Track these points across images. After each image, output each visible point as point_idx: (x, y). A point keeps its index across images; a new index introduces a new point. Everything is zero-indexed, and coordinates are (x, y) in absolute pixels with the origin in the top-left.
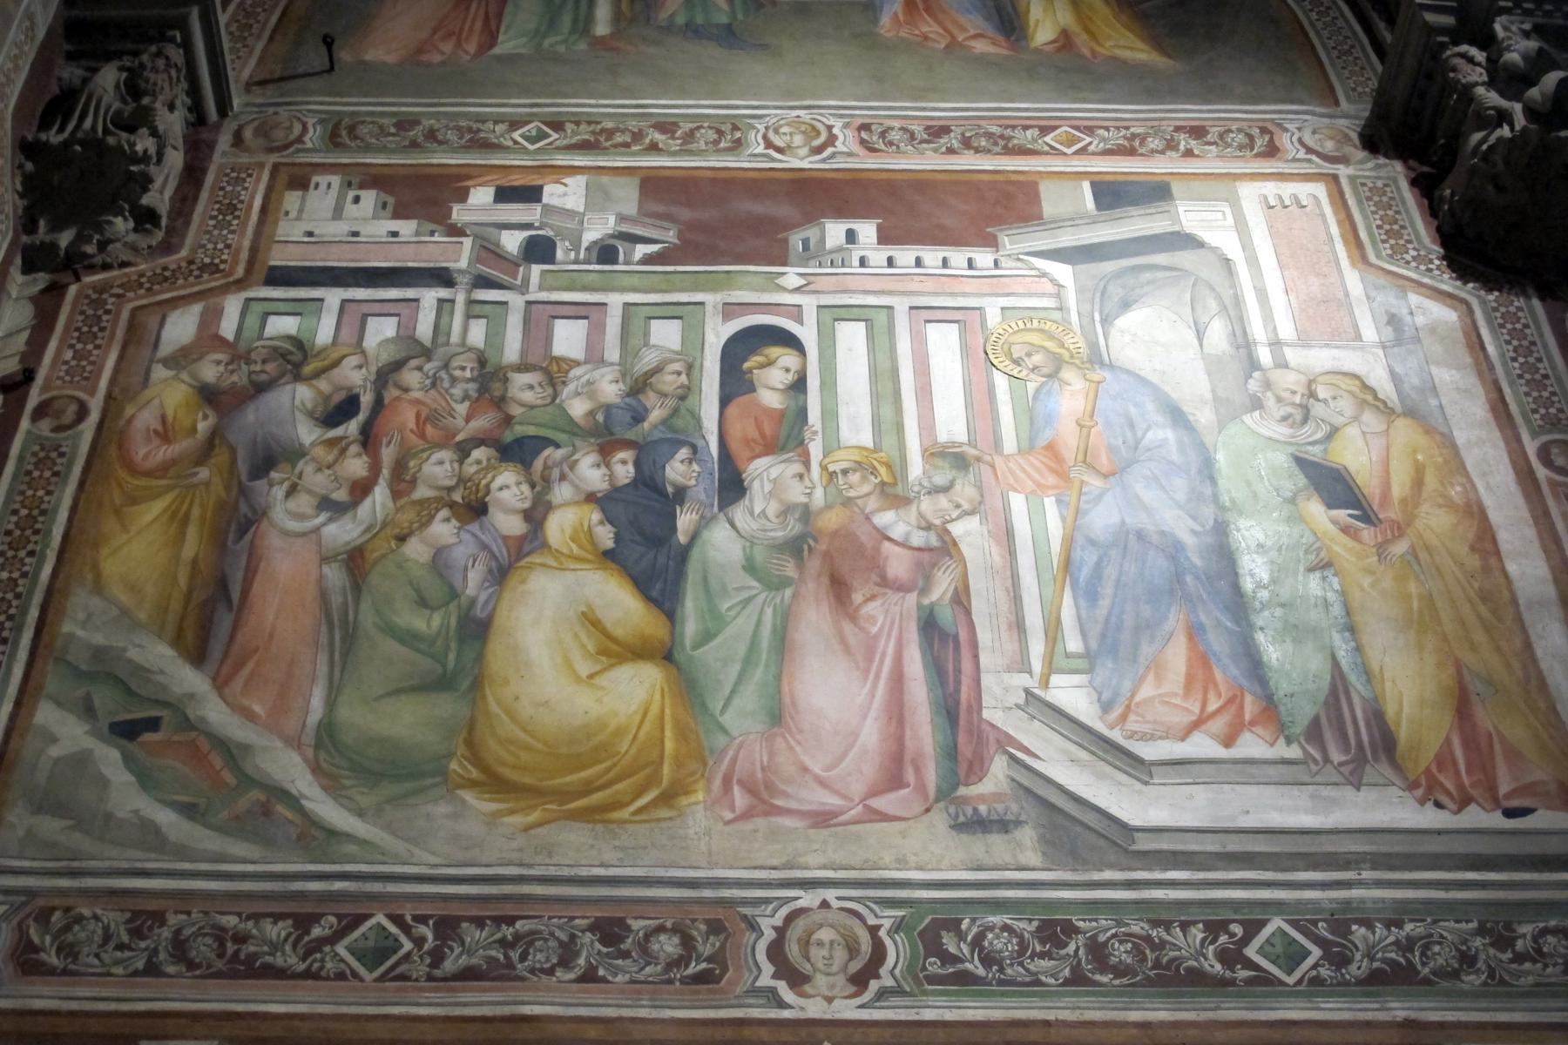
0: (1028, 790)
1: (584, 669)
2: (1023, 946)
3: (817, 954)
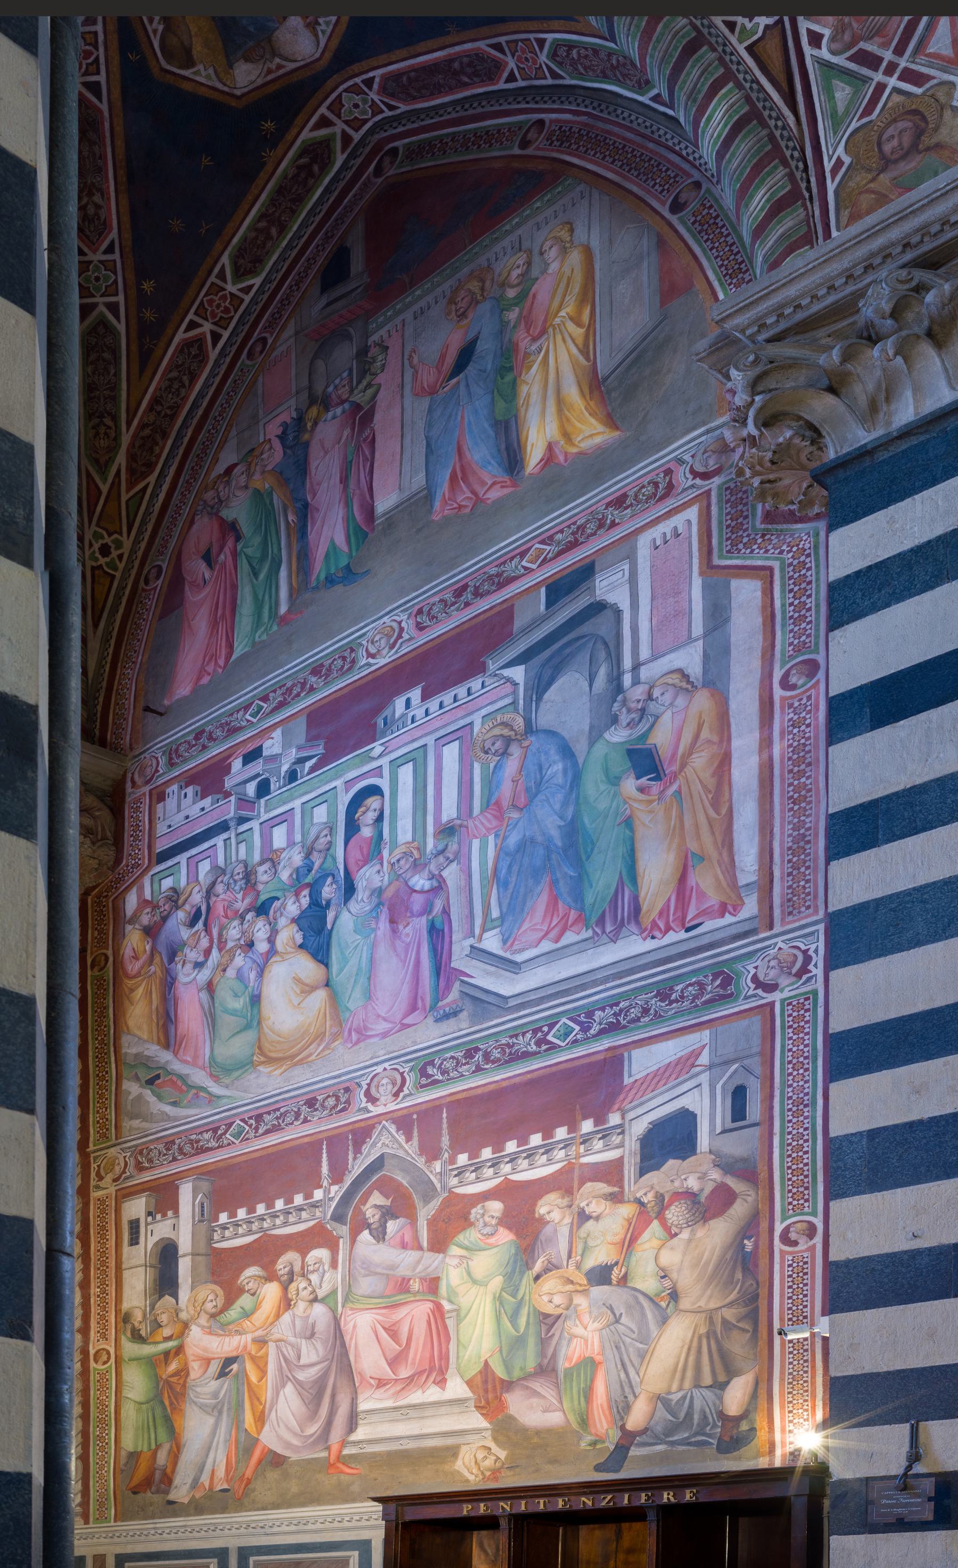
0: (467, 994)
1: (296, 1001)
2: (458, 1063)
3: (381, 1089)
